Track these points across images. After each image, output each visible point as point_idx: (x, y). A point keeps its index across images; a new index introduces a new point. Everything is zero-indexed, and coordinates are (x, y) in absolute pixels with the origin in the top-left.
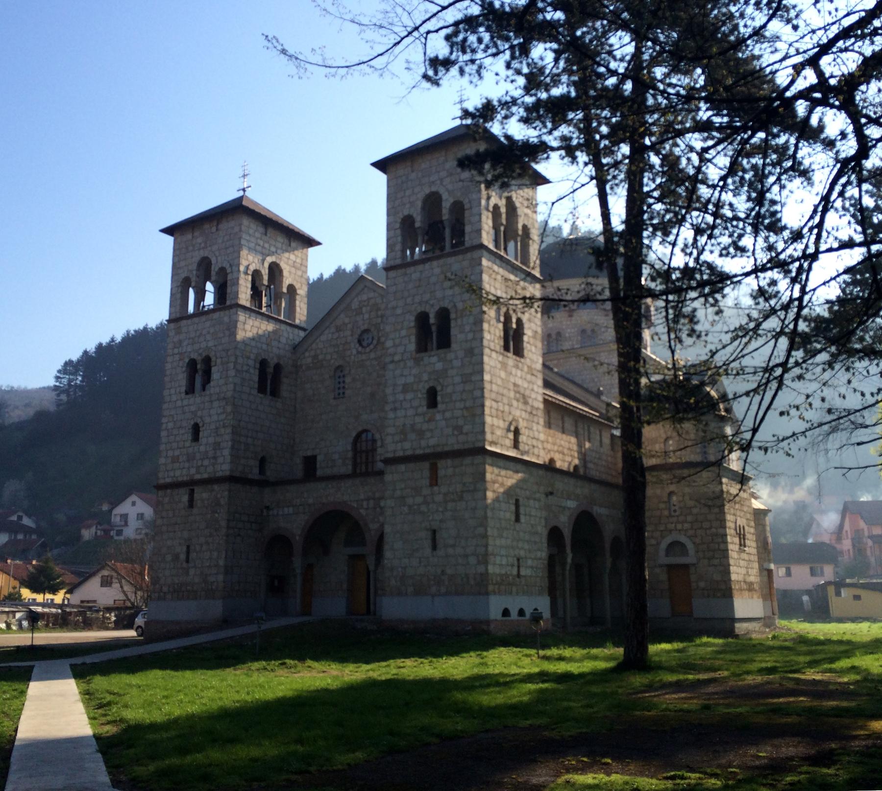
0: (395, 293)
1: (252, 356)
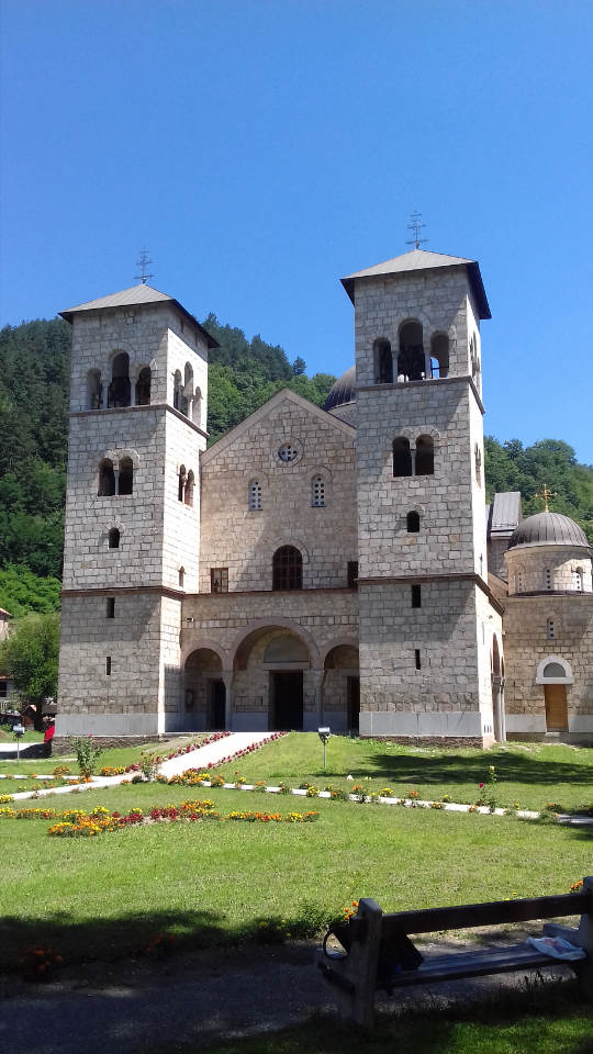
0: (367, 414)
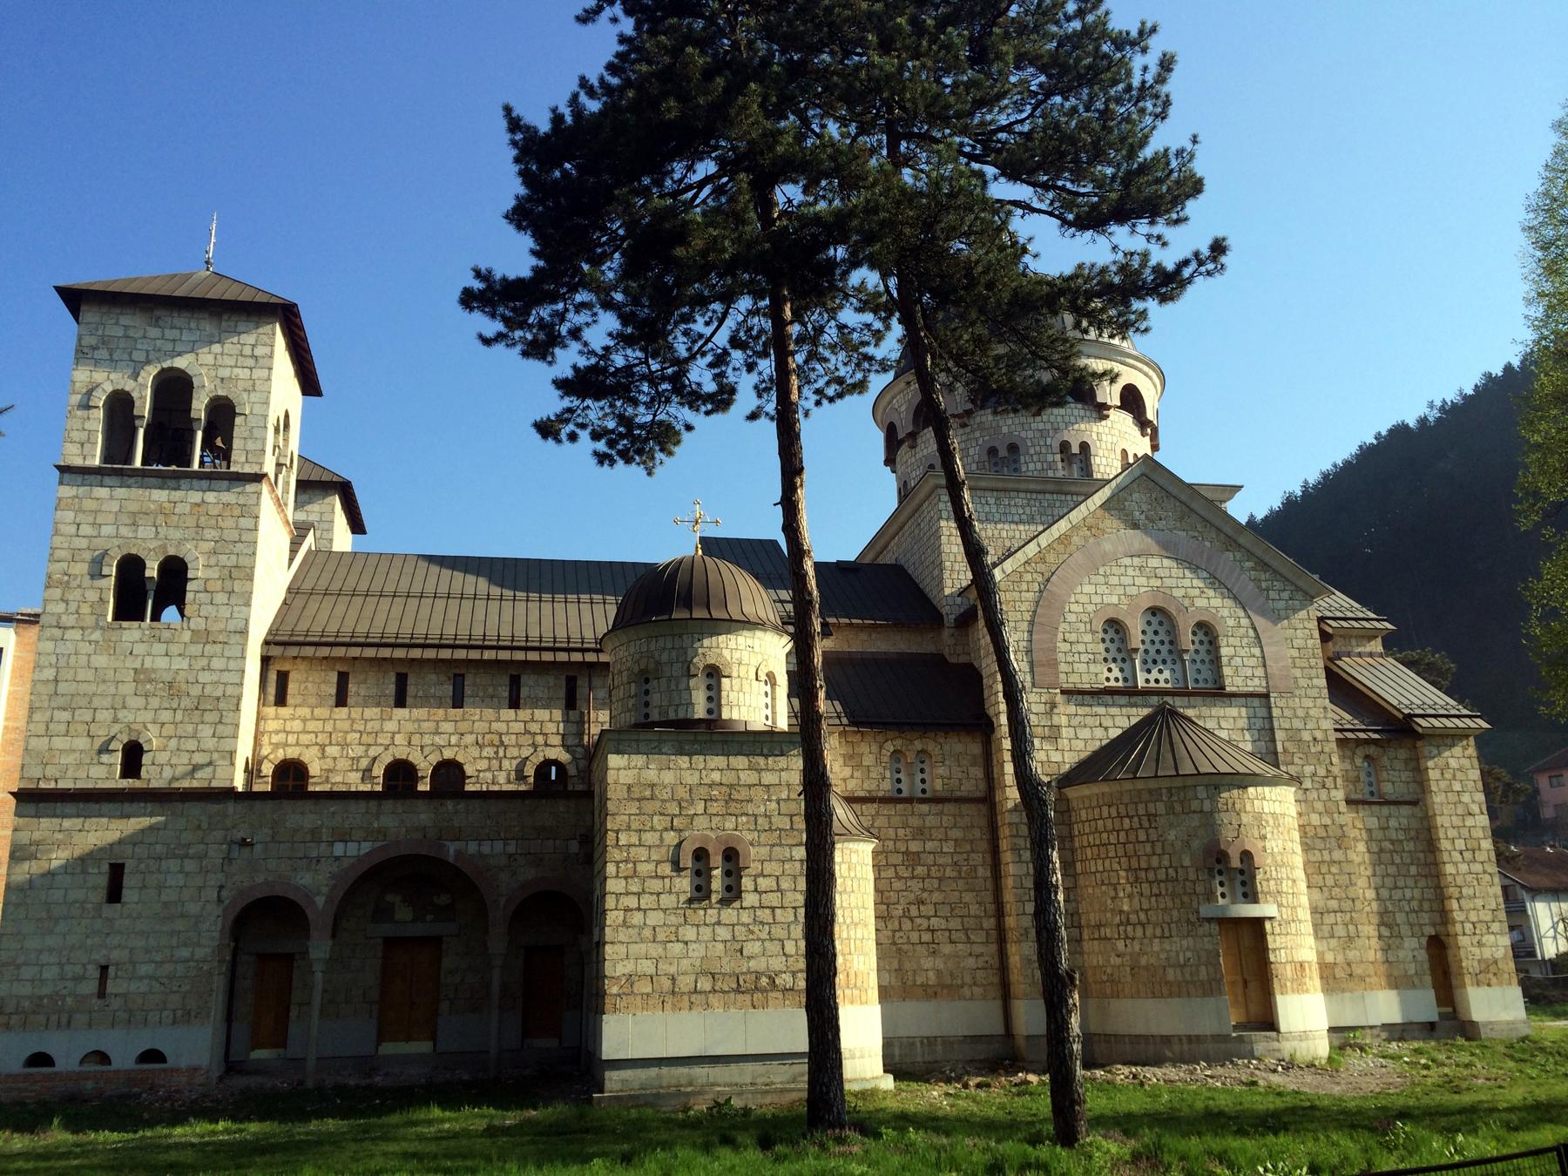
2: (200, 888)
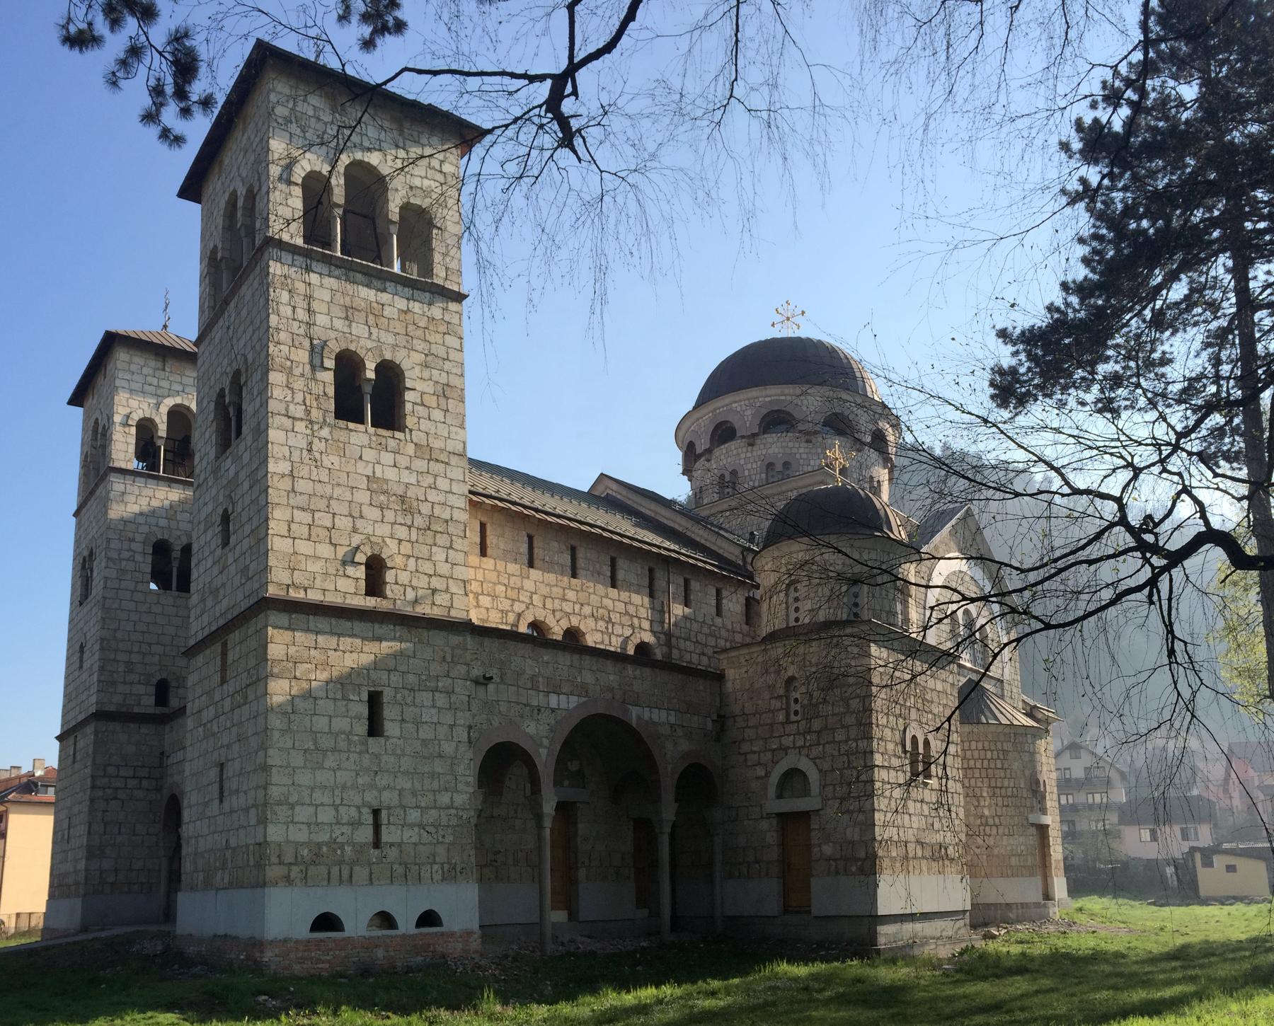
1: (139, 538)
2: (451, 727)
